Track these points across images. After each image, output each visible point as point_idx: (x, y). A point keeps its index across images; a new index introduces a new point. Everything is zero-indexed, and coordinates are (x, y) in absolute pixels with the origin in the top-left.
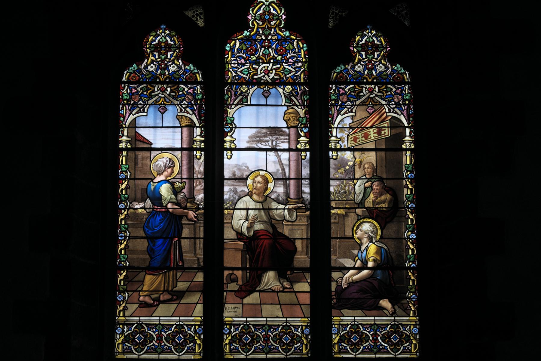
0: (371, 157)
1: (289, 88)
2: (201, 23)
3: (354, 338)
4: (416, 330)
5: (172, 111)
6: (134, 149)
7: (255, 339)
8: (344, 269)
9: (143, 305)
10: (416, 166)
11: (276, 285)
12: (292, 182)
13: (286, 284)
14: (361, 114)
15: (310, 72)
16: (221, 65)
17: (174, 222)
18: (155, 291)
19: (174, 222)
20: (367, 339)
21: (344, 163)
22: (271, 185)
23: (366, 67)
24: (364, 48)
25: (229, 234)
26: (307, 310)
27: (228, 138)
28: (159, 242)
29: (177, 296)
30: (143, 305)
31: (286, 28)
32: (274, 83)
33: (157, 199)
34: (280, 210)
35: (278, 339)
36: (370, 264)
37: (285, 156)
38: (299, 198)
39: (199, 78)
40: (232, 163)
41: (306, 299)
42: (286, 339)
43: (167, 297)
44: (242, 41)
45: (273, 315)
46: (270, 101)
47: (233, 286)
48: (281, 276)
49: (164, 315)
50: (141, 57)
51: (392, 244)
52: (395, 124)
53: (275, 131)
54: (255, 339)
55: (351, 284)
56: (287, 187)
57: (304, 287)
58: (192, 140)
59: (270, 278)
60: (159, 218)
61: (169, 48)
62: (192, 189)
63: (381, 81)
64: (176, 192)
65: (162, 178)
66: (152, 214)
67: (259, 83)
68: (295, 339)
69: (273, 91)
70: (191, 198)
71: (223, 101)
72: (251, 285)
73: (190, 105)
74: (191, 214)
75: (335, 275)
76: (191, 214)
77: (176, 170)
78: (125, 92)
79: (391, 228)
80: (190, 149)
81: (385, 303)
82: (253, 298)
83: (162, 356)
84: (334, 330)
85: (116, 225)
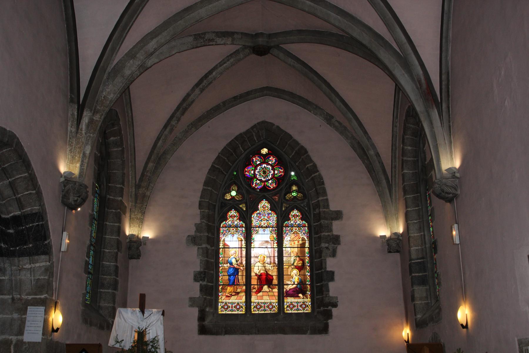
0: (296, 250)
1: (271, 229)
2: (244, 209)
3: (291, 306)
4: (310, 304)
5: (236, 236)
6: (224, 248)
7: (261, 307)
8: (288, 285)
9: (227, 296)
10: (310, 252)
11: (267, 290)
12: (272, 258)
13: (270, 290)
14: (293, 236)
15: (277, 224)
16: (251, 221)
17: (236, 270)
18: (231, 292)
19: (236, 270)
20: (295, 306)
21: (288, 252)
22: (266, 259)
23: (294, 222)
24: (294, 216)
25: (253, 274)
26: (277, 298)
27: (252, 245)
28: (232, 277)
29: (238, 293)
30: (227, 296)
31: (270, 210)
32: (266, 227)
33: (231, 264)
34: (268, 267)
35: (268, 307)
36: (296, 283)
37: (270, 249)
38: (274, 263)
39: (244, 225)
40: (254, 252)
41: (276, 294)
42: (271, 307)
43: (234, 294)
44: (257, 214)
45: (266, 299)
46: (266, 232)
47: (254, 290)
48: (269, 287)
49: (233, 299)
50: (226, 219)
51: (302, 277)
52: (303, 239)
53: (267, 242)
54: (261, 307)
55: (290, 289)
56: (270, 259)
57: (276, 290)
58: (242, 245)
59: (265, 288)
60: (232, 269)
61: (235, 216)
62: (242, 260)
63: (299, 226)
64: (237, 261)
65: (233, 257)
66: (230, 268)
67: (262, 227)
68: (273, 307)
69: (266, 229)
70: (242, 263)
71: (251, 233)
72: (260, 290)
73: (241, 234)
74: (242, 268)
75: (285, 286)
76: (242, 268)
77: (237, 254)
78: (222, 230)
79: (302, 272)
80: (241, 248)
81: (300, 295)
82: (260, 294)
83: (233, 313)
84: (285, 304)
85: (219, 272)
